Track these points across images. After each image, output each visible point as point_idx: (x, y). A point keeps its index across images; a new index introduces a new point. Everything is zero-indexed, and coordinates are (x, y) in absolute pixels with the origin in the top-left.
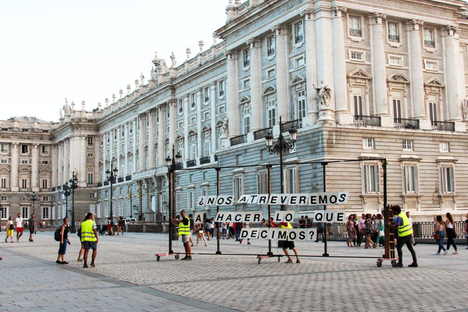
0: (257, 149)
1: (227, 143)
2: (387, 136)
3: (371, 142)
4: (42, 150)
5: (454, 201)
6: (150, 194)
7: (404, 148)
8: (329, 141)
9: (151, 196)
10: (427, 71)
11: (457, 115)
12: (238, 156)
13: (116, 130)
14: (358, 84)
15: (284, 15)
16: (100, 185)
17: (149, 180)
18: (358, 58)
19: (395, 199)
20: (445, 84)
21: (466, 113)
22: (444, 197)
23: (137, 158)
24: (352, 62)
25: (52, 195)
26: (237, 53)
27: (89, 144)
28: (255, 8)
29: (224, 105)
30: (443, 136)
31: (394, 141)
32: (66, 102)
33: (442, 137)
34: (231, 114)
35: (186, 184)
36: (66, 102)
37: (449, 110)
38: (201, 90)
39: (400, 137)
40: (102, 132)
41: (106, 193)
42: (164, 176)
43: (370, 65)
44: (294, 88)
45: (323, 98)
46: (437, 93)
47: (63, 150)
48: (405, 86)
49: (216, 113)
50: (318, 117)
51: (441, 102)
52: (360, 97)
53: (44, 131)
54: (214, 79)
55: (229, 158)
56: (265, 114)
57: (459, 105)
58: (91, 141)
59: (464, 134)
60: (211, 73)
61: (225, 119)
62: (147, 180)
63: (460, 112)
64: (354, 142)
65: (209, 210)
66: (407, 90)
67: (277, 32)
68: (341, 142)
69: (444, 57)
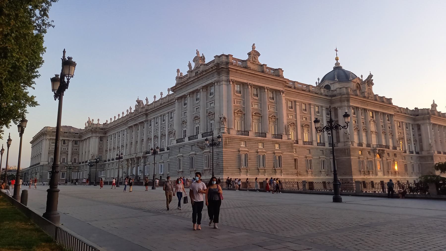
0: (190, 145)
1: (175, 142)
2: (251, 141)
4: (74, 144)
6: (133, 166)
8: (225, 142)
9: (133, 167)
12: (180, 148)
13: (115, 134)
15: (205, 82)
16: (105, 161)
17: (132, 159)
23: (126, 148)
24: (236, 106)
25: (78, 166)
26: (181, 99)
27: (101, 140)
28: (191, 78)
29: (172, 124)
31: (255, 143)
32: (89, 119)
34: (176, 127)
35: (152, 161)
36: (89, 119)
38: (161, 116)
40: (108, 135)
41: (109, 165)
42: (140, 157)
44: (209, 117)
45: (223, 122)
46: (274, 121)
47: (86, 143)
48: (260, 117)
49: (168, 127)
50: (220, 131)
51: (276, 126)
53: (76, 133)
54: (168, 111)
55: (175, 149)
56: (194, 129)
58: (102, 139)
60: (166, 108)
61: (174, 130)
62: (131, 159)
64: (237, 143)
65: (163, 174)
67: (201, 90)
68: (231, 143)
69: (278, 105)
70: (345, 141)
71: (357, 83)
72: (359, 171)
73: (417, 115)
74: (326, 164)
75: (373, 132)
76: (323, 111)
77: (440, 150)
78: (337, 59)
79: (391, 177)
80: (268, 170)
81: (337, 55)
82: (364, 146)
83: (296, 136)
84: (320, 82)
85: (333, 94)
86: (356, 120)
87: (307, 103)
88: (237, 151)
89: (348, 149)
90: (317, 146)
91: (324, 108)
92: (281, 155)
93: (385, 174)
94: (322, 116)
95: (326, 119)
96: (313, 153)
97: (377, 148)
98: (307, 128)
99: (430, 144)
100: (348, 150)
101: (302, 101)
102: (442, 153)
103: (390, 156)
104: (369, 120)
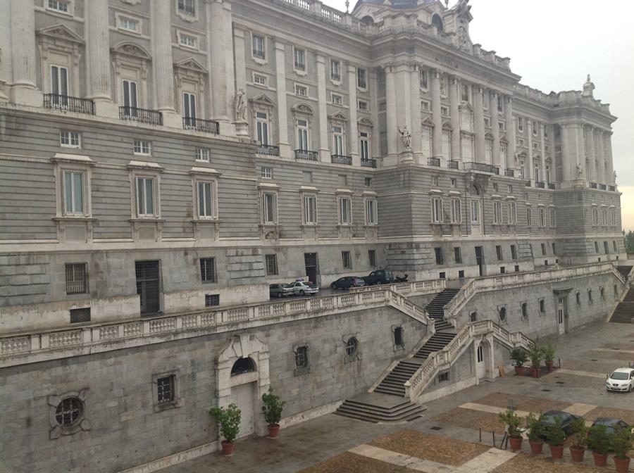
2: (107, 131)
3: (77, 137)
5: (215, 229)
7: (136, 151)
10: (181, 48)
11: (225, 113)
14: (60, 48)
18: (61, 9)
19: (117, 224)
20: (209, 69)
21: (238, 113)
22: (200, 223)
30: (201, 139)
31: (119, 139)
33: (198, 139)
37: (213, 106)
39: (130, 135)
43: (83, 23)
46: (197, 82)
48: (144, 63)
51: (202, 94)
52: (64, 71)
57: (228, 101)
59: (231, 140)
63: (229, 110)
64: (43, 136)
66: (147, 71)
69: (208, 32)
76: (350, 74)
77: (594, 181)
79: (497, 237)
80: (168, 225)
83: (273, 136)
88: (42, 161)
90: (332, 162)
91: (354, 66)
92: (214, 181)
94: (345, 86)
95: (357, 97)
96: (319, 181)
97: (472, 171)
98: (307, 116)
99: (578, 168)
100: (404, 174)
101: (293, 40)
102: (598, 186)
104: (459, 104)
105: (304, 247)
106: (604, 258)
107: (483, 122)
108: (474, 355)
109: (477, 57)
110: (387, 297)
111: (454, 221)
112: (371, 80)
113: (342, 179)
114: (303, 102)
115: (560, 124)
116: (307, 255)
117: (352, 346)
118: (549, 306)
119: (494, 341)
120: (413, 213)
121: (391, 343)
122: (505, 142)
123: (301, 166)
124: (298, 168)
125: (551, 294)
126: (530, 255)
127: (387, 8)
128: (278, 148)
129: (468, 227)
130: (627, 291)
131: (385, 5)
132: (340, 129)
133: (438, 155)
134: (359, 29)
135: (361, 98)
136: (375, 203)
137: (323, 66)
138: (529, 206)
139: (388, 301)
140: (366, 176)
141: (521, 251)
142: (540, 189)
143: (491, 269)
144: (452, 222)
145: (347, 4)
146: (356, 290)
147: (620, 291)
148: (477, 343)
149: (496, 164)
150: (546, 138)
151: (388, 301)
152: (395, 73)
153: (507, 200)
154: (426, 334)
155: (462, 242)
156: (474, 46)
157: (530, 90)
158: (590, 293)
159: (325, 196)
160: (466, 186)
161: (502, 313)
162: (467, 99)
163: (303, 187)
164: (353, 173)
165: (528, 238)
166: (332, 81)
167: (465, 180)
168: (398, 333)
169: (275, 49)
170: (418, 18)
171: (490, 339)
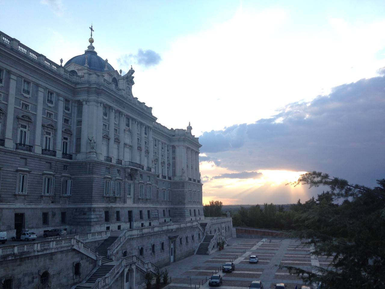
70: (88, 151)
71: (113, 77)
72: (102, 196)
73: (174, 136)
74: (53, 185)
75: (126, 145)
76: (60, 102)
77: (190, 177)
78: (91, 41)
79: (141, 205)
81: (91, 35)
82: (114, 162)
84: (63, 65)
85: (79, 81)
86: (107, 125)
87: (32, 82)
89: (91, 164)
91: (63, 97)
93: (135, 201)
94: (56, 108)
96: (31, 165)
97: (130, 167)
99: (183, 169)
100: (90, 165)
101: (23, 75)
102: (192, 179)
103: (143, 179)
104: (125, 128)
105: (14, 209)
106: (194, 219)
107: (137, 140)
108: (124, 279)
109: (136, 105)
110: (72, 243)
111: (117, 195)
112: (73, 107)
113: (48, 165)
114: (26, 114)
115: (175, 146)
116: (17, 215)
117: (45, 277)
118: (166, 248)
119: (136, 268)
120: (93, 189)
121: (71, 275)
122: (147, 152)
123: (20, 154)
124: (17, 155)
125: (167, 238)
126: (157, 216)
127: (86, 68)
128: (4, 141)
129: (125, 199)
130: (205, 237)
131: (85, 67)
132: (50, 133)
133: (111, 155)
134: (68, 77)
135: (66, 117)
136: (69, 182)
137: (43, 94)
138: (158, 188)
139: (73, 246)
140: (65, 164)
141: (153, 214)
142: (164, 179)
143: (136, 224)
144: (116, 196)
145: (62, 61)
146: (51, 238)
147: (201, 237)
148: (126, 270)
149: (142, 164)
150: (168, 152)
151: (73, 246)
152: (88, 105)
153: (147, 184)
154: (95, 266)
155: (121, 208)
156: (134, 98)
157: (161, 126)
158: (187, 238)
159: (35, 175)
160: (125, 174)
161: (141, 251)
162: (128, 126)
163: (19, 168)
164: (56, 161)
165: (157, 206)
166: (48, 103)
167: (125, 172)
168: (77, 268)
169: (10, 78)
170: (104, 78)
171: (134, 267)
